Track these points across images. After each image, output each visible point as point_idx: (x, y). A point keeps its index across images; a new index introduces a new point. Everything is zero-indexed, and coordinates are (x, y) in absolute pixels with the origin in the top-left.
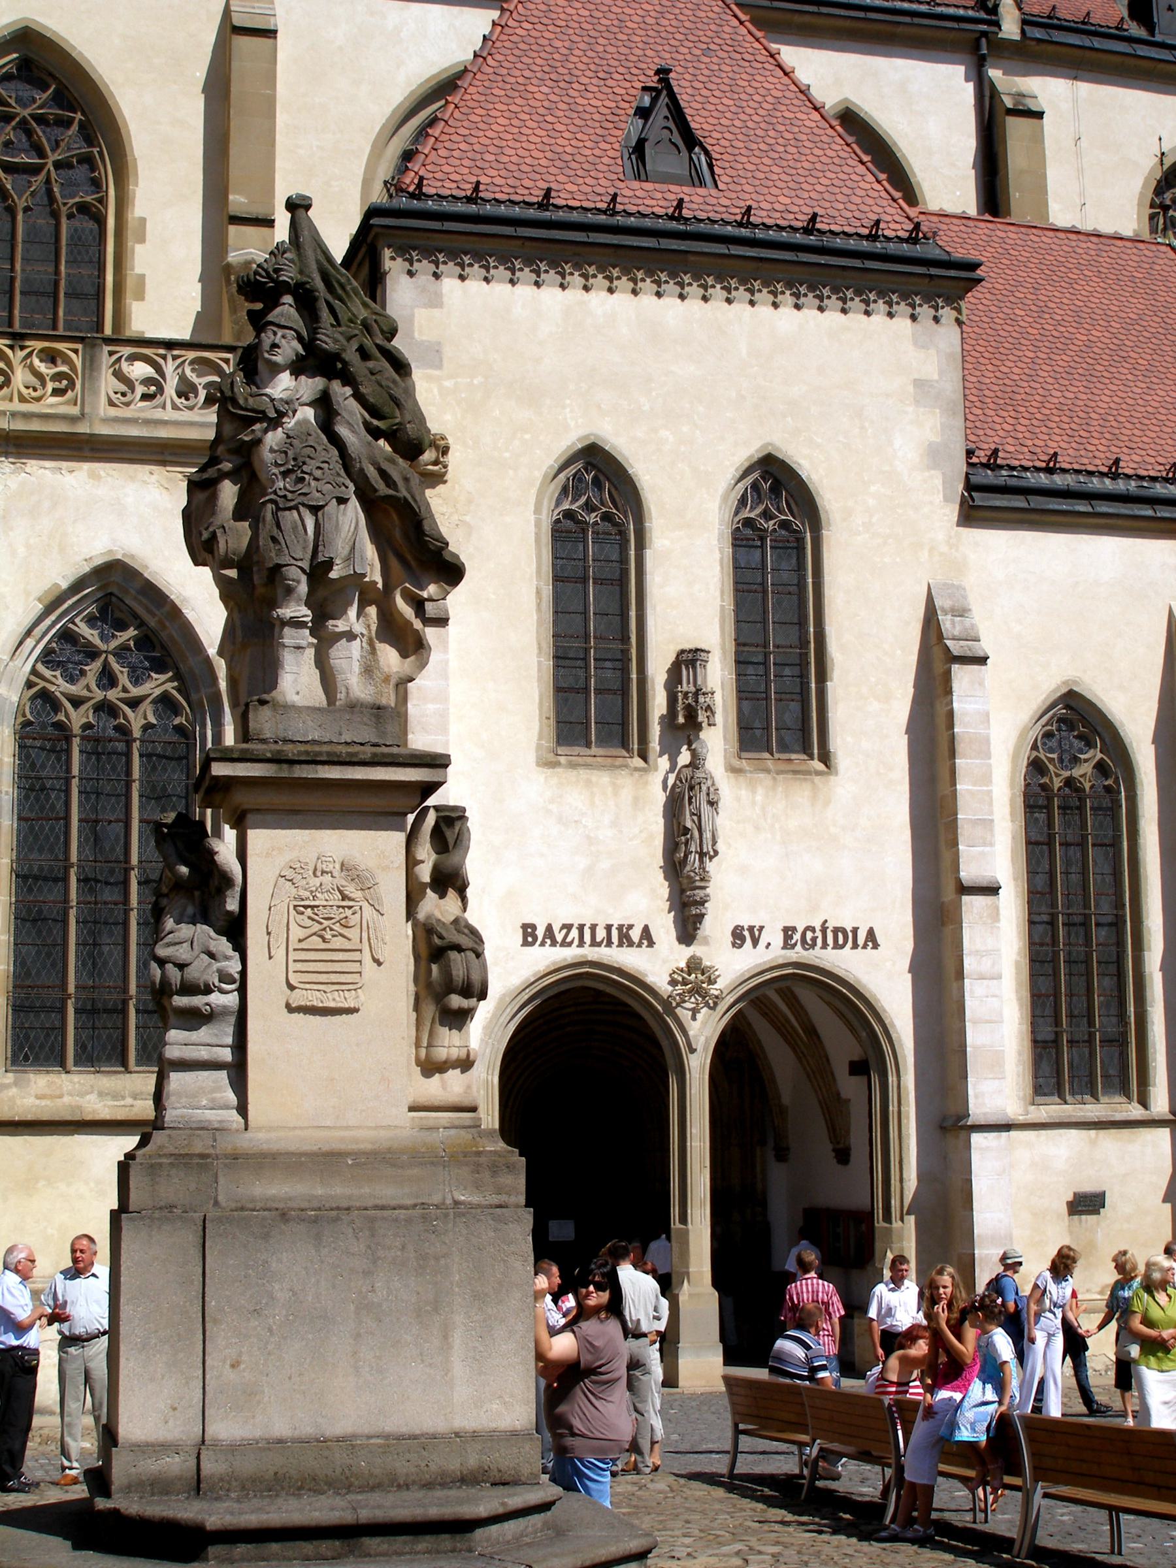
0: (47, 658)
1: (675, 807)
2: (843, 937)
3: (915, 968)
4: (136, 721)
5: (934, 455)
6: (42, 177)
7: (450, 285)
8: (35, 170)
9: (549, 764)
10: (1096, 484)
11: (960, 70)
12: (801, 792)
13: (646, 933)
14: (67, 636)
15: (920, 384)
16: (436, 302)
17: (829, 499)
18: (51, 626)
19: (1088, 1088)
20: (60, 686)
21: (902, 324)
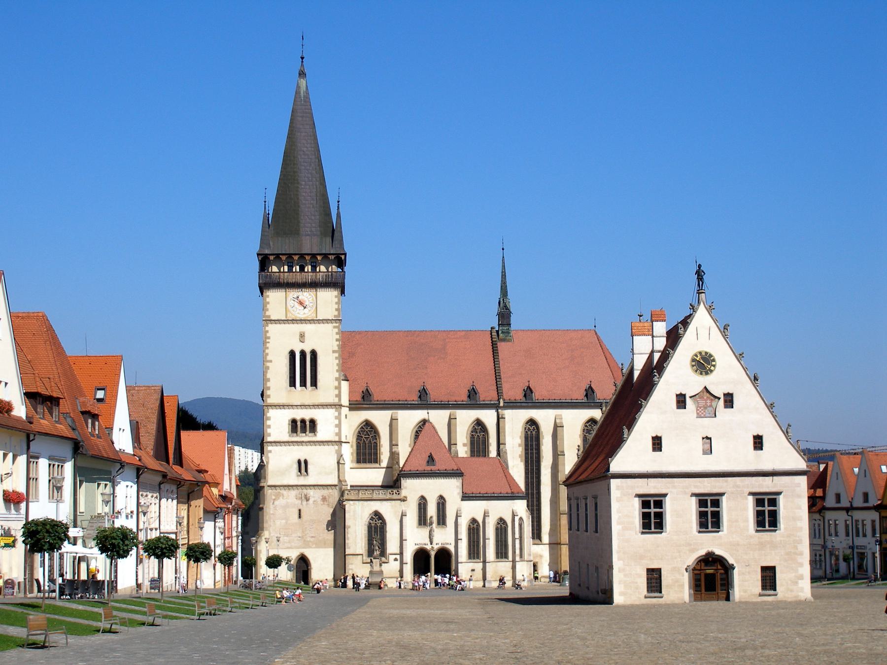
0: (370, 519)
1: (430, 532)
2: (447, 544)
3: (455, 547)
4: (378, 525)
5: (459, 493)
6: (369, 439)
7: (408, 480)
8: (369, 438)
9: (418, 528)
10: (477, 495)
11: (494, 411)
12: (443, 529)
13: (427, 544)
14: (372, 517)
15: (457, 486)
16: (406, 482)
17: (447, 499)
18: (371, 516)
19: (474, 558)
20: (372, 522)
21: (455, 480)
